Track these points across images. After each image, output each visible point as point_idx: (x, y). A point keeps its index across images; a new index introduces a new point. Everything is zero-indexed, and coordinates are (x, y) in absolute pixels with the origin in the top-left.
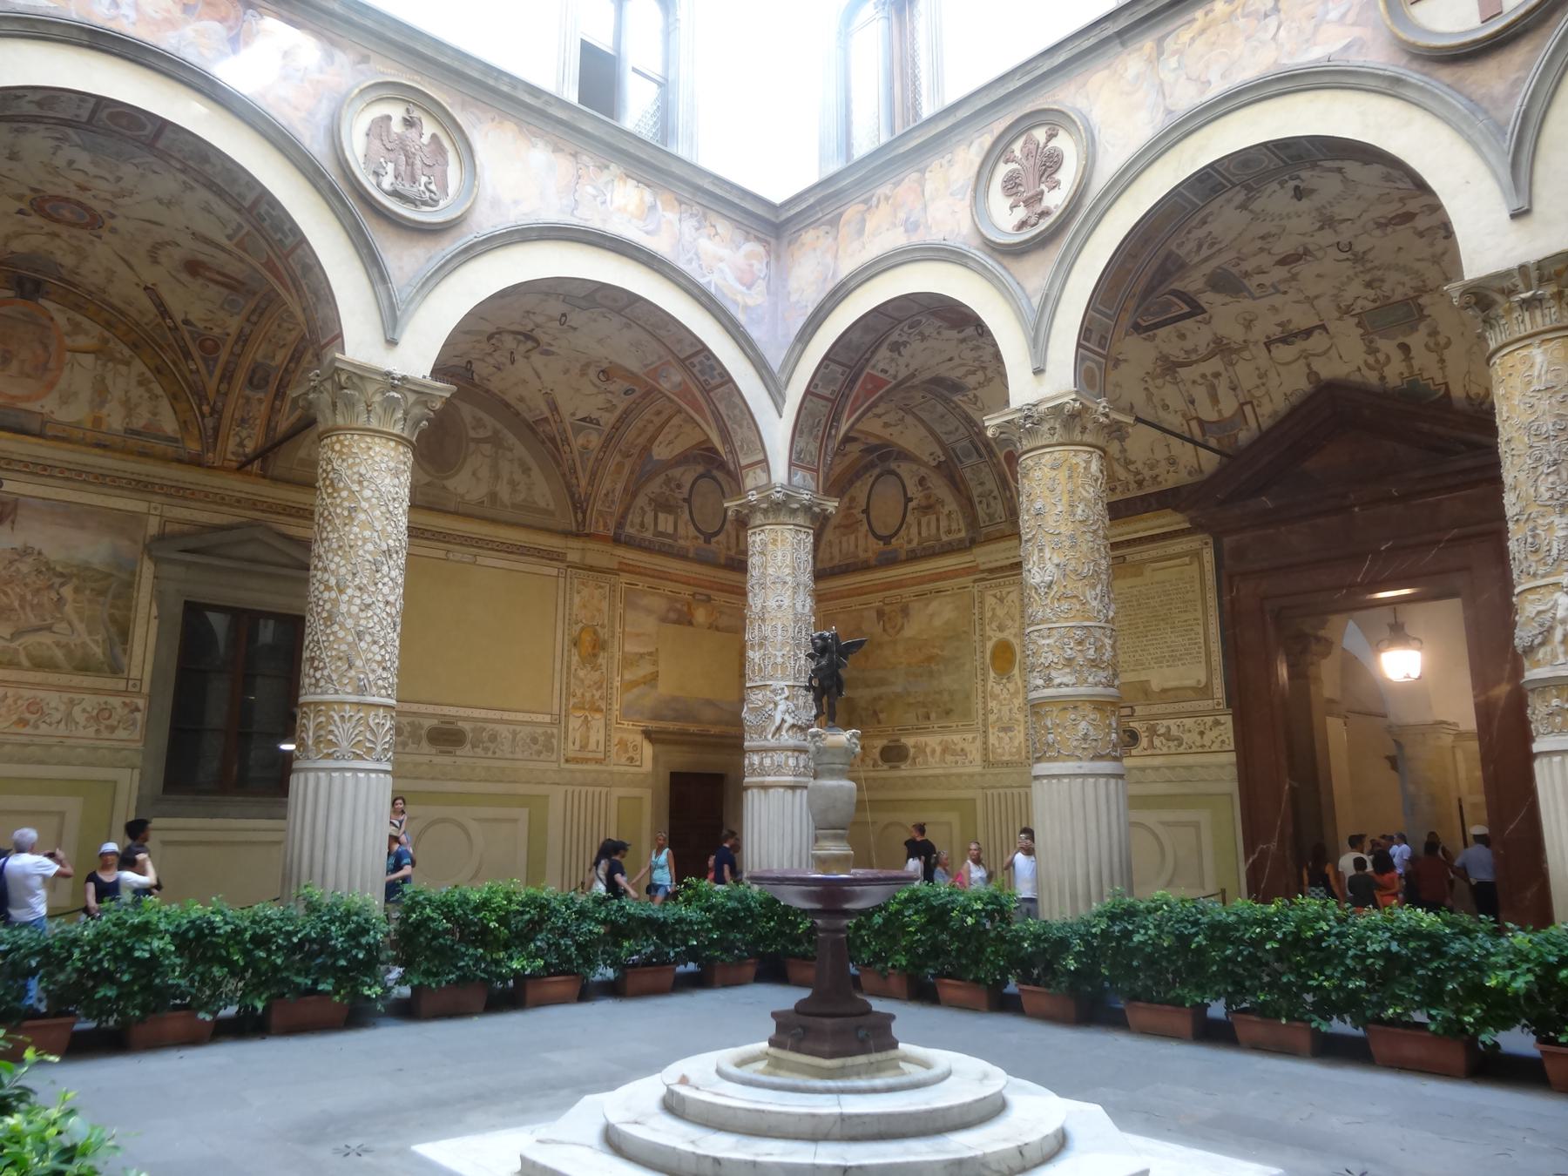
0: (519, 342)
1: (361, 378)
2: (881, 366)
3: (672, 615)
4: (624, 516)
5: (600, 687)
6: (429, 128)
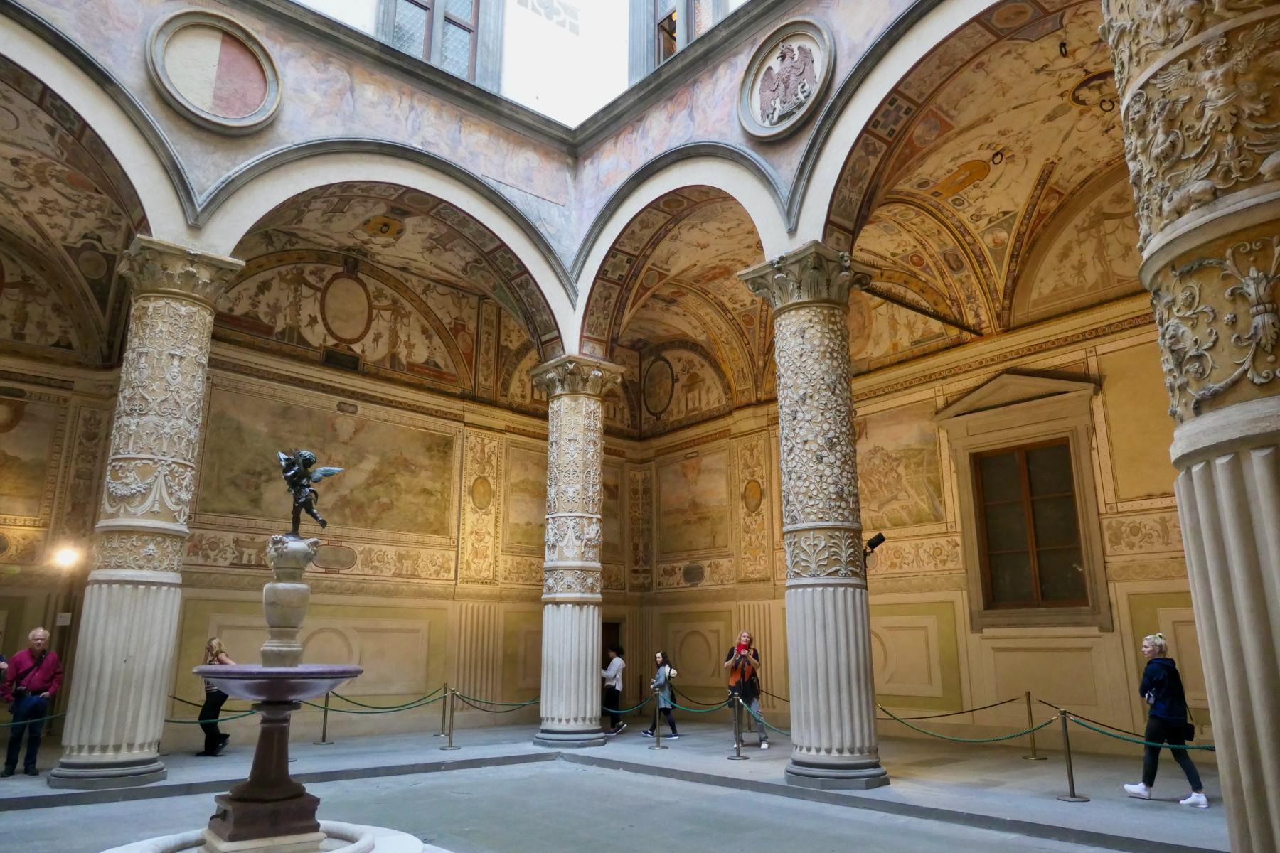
0: (1099, 87)
1: (762, 277)
6: (795, 45)
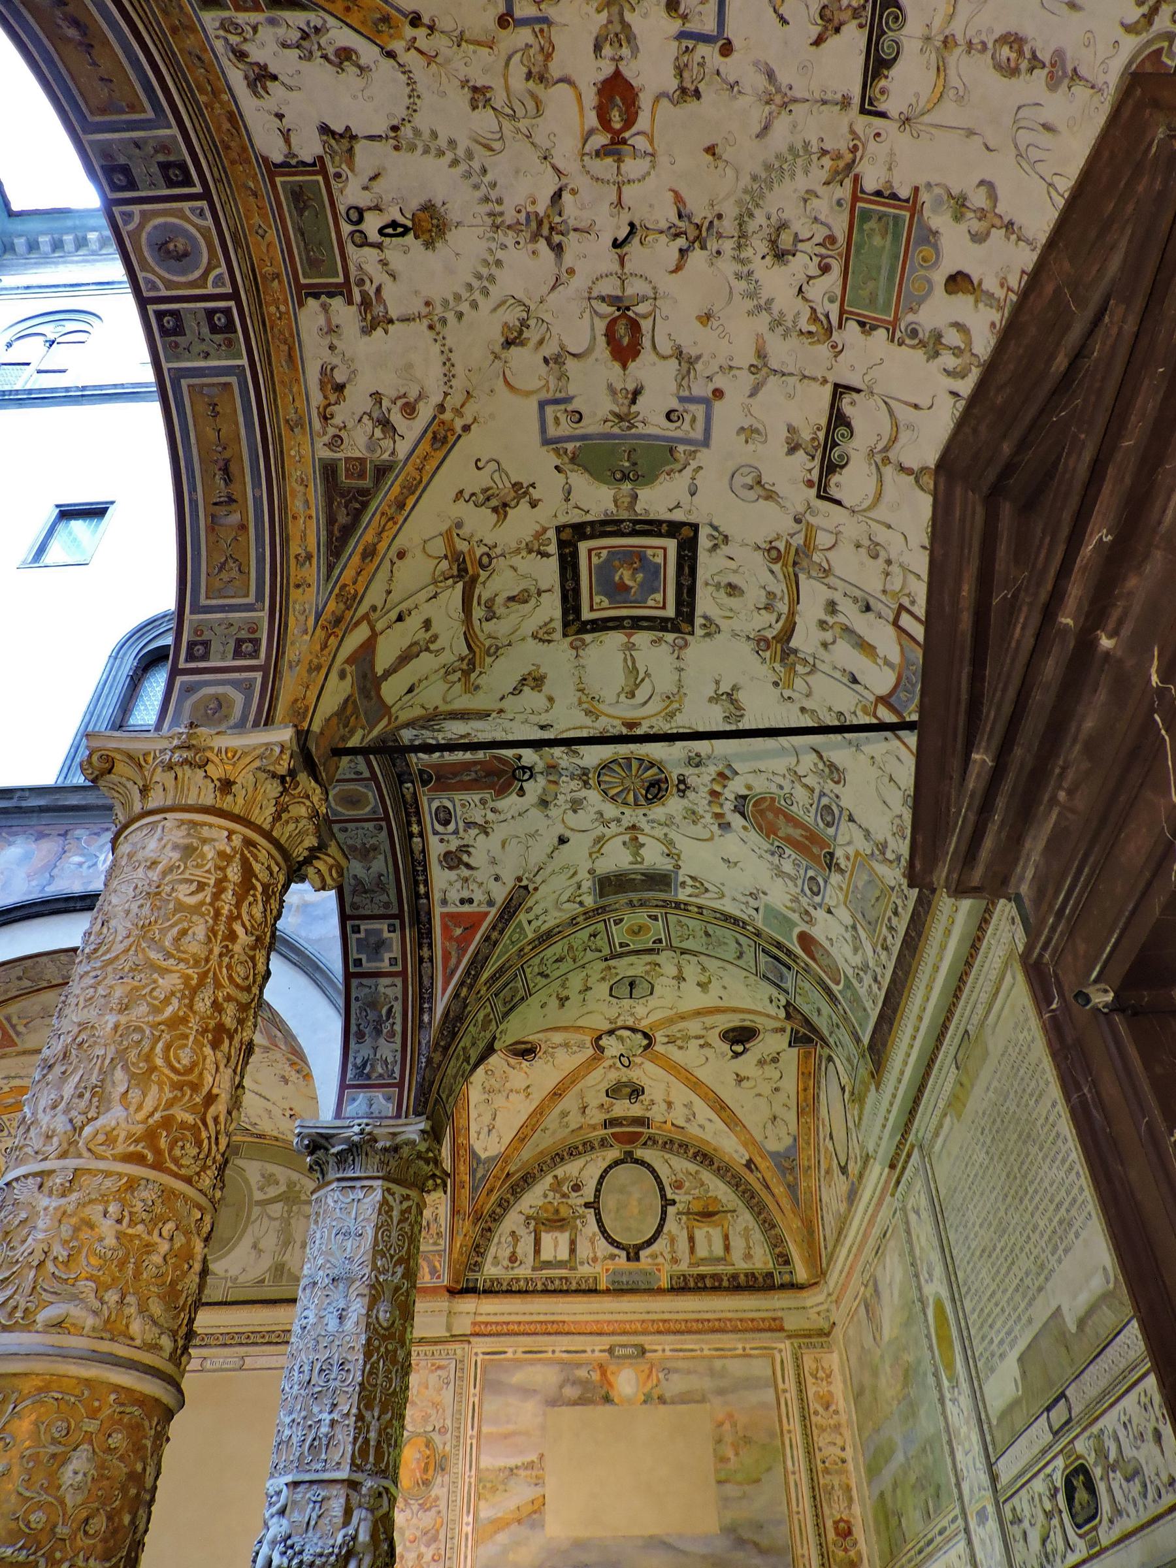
2: (454, 895)
3: (570, 1392)
4: (479, 1249)
5: (435, 1539)
